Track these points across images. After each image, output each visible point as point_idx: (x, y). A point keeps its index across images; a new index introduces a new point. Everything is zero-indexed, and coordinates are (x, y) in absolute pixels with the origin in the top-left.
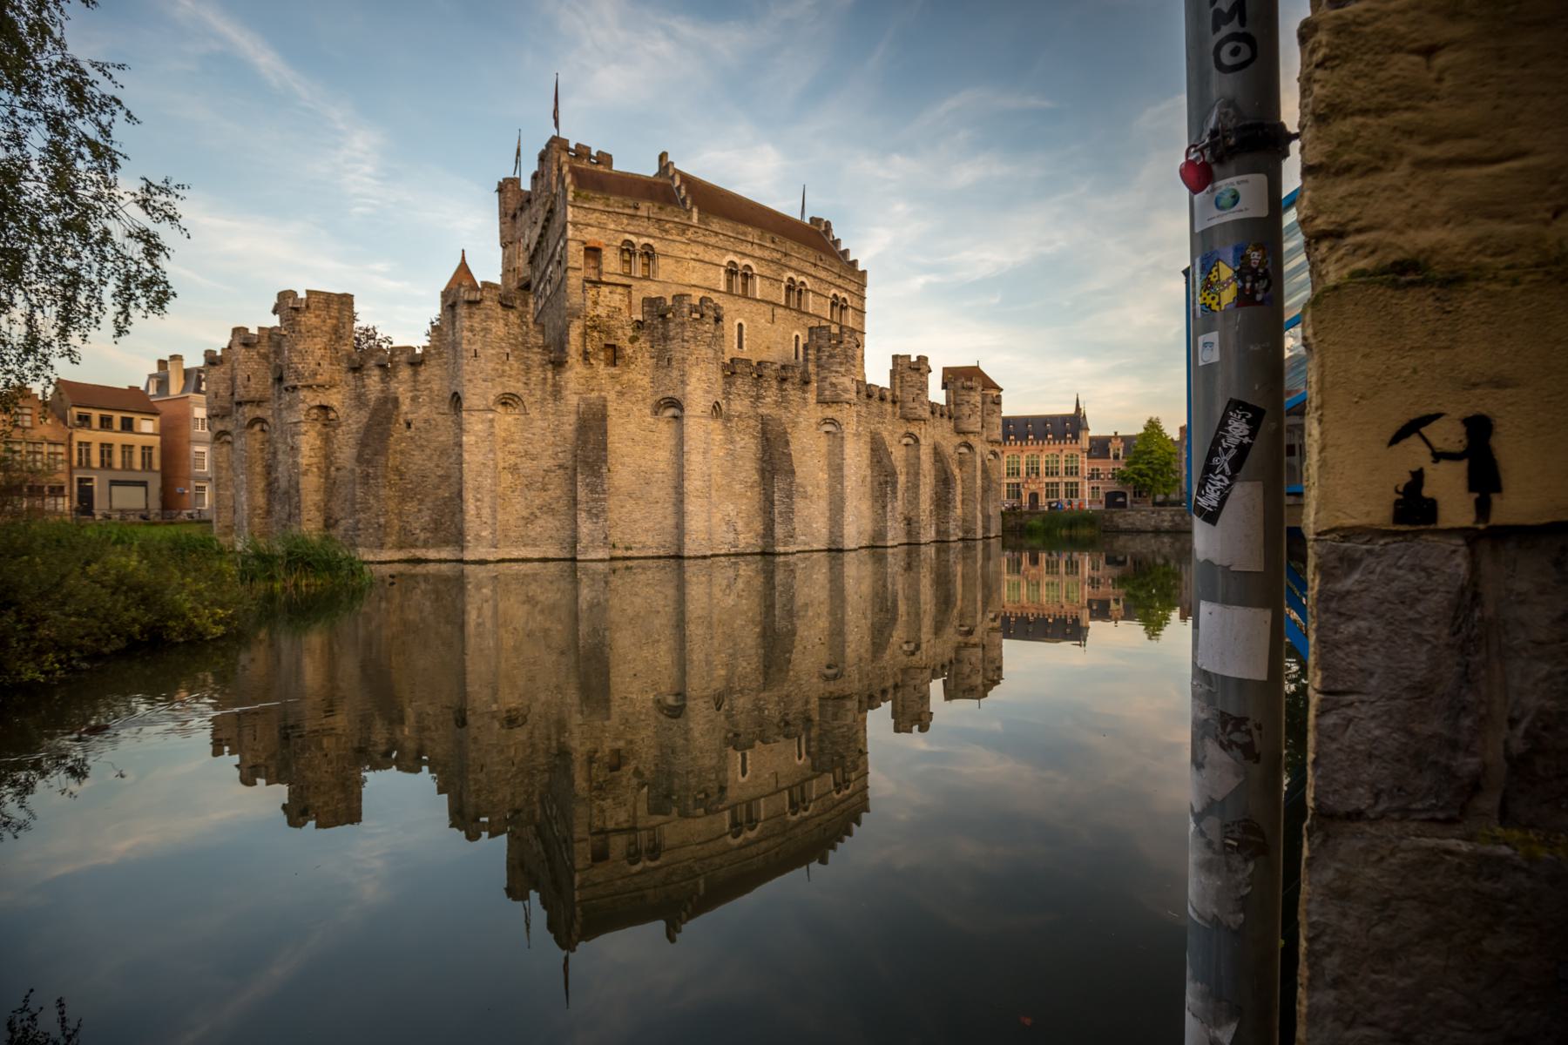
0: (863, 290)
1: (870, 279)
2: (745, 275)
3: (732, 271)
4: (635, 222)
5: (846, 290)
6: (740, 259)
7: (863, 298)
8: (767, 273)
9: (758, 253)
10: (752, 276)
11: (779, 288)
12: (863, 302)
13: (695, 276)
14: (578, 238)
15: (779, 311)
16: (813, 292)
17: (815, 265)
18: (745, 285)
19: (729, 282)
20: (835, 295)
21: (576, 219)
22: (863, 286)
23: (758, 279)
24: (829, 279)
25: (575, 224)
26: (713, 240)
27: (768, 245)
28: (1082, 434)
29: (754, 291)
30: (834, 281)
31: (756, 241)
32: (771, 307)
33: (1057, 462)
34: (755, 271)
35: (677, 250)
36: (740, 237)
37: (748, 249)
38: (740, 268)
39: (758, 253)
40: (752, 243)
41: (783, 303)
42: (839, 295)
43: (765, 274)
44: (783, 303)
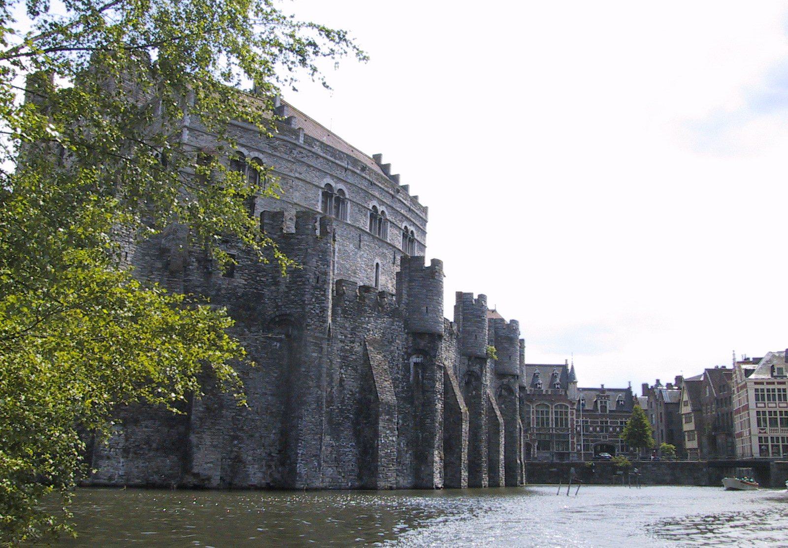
0: (425, 225)
1: (431, 217)
2: (338, 200)
3: (328, 193)
4: (246, 136)
5: (414, 224)
6: (336, 183)
7: (424, 233)
8: (357, 199)
9: (351, 179)
10: (343, 202)
11: (365, 215)
12: (425, 236)
13: (297, 194)
14: (192, 144)
15: (366, 238)
16: (391, 222)
17: (393, 197)
18: (337, 208)
19: (324, 203)
20: (406, 227)
21: (194, 125)
22: (425, 222)
23: (349, 205)
24: (402, 211)
25: (190, 129)
26: (312, 162)
27: (358, 172)
28: (571, 386)
29: (345, 218)
30: (405, 213)
31: (350, 167)
32: (359, 232)
33: (547, 412)
34: (347, 196)
35: (284, 167)
36: (337, 161)
37: (342, 175)
38: (336, 192)
39: (351, 179)
40: (346, 169)
41: (368, 230)
42: (409, 227)
43: (355, 200)
44: (368, 230)
